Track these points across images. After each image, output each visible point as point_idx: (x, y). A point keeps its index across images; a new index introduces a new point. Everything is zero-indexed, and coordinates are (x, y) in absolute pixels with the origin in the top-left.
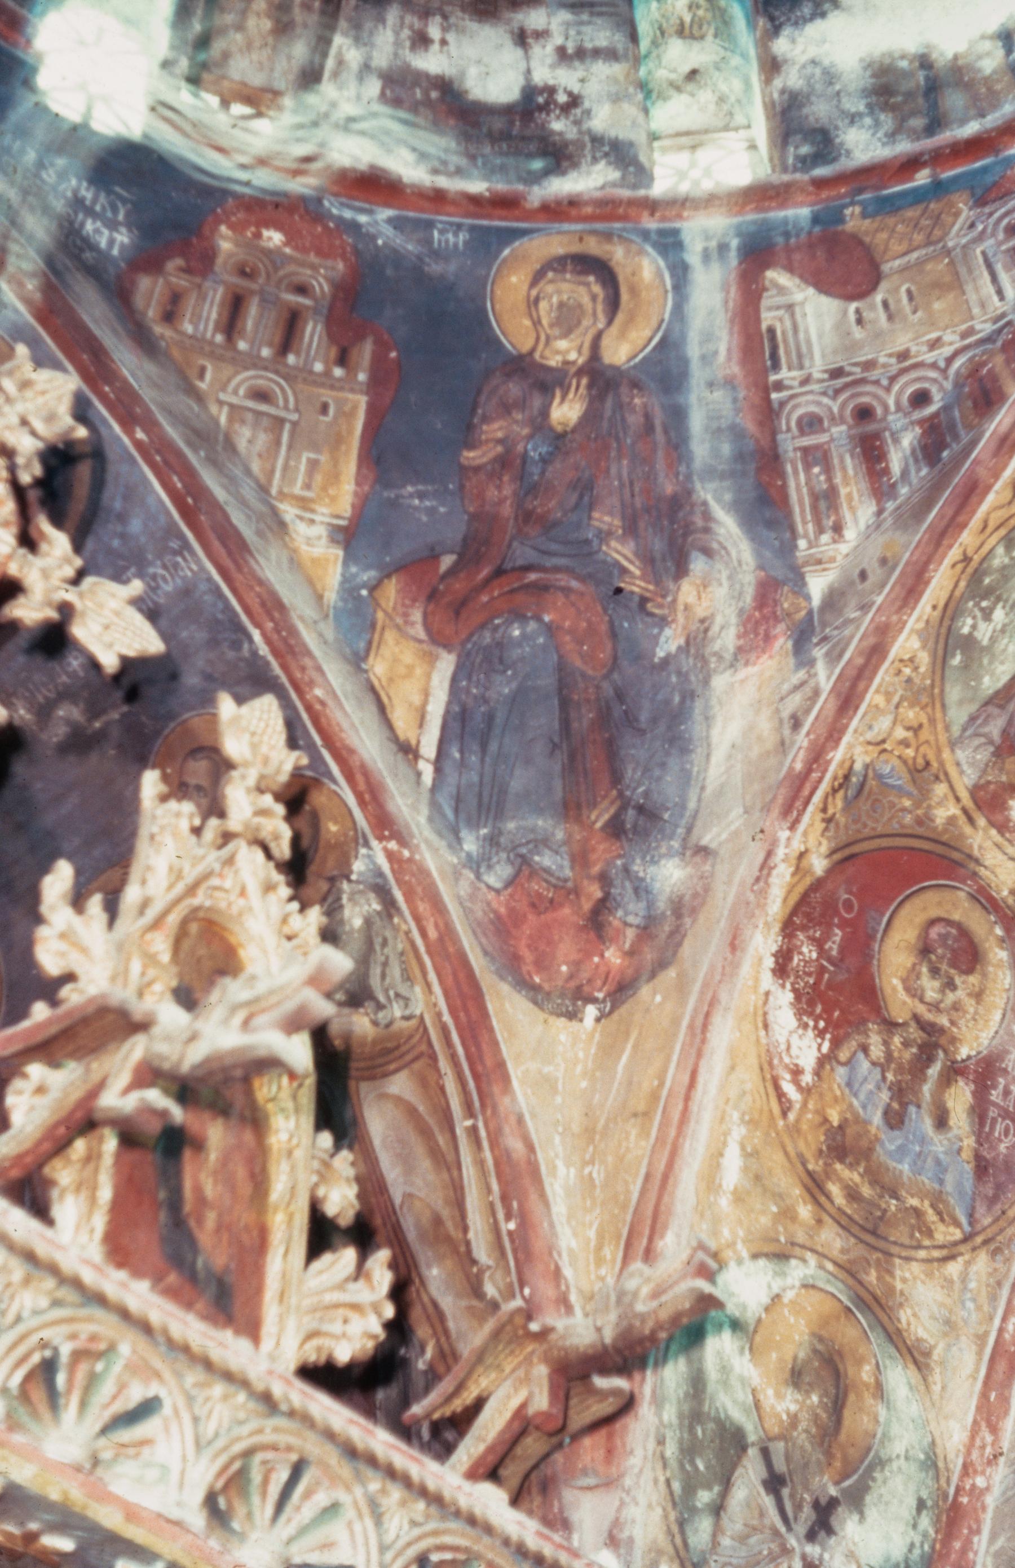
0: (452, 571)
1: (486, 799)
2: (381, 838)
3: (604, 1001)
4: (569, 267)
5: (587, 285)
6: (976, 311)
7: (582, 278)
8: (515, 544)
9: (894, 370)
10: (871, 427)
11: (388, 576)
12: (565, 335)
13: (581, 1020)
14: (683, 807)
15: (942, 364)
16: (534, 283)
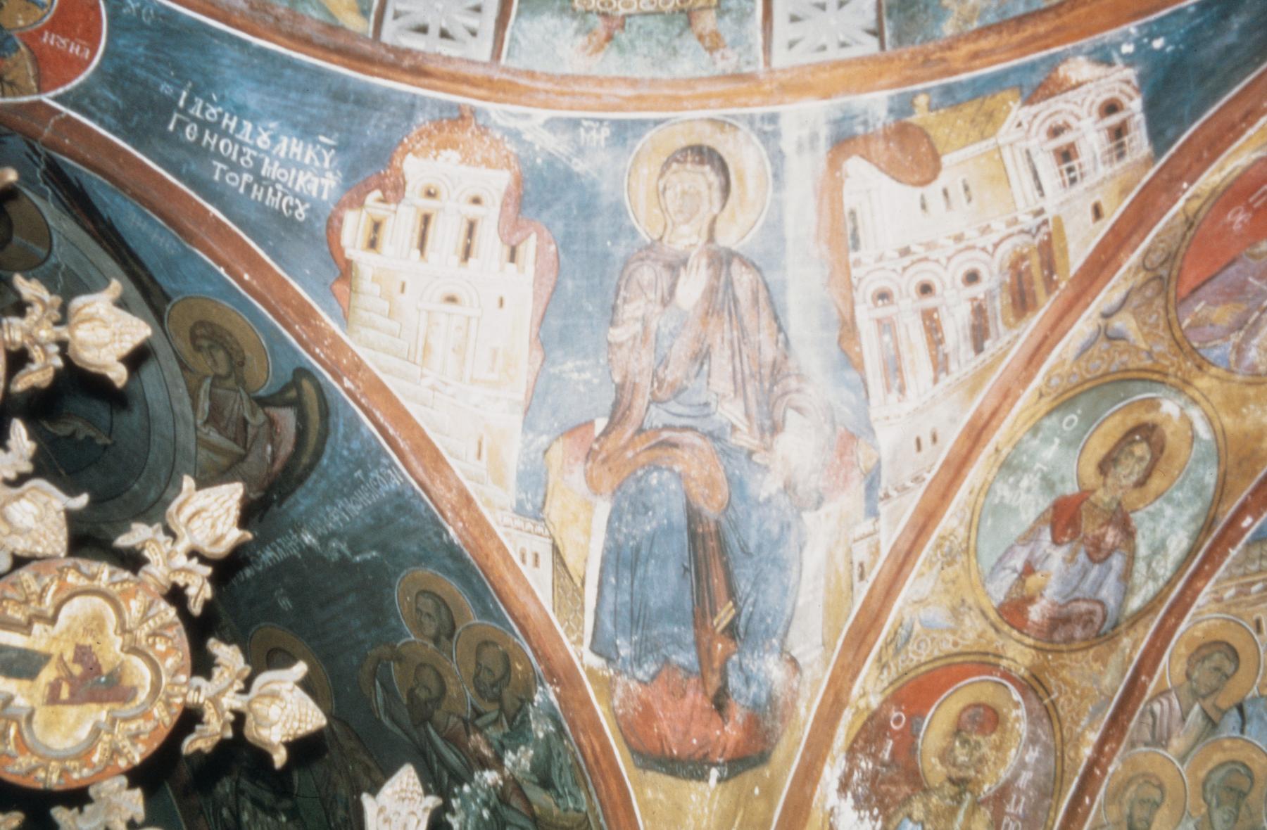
0: (606, 433)
1: (636, 614)
2: (552, 683)
3: (723, 765)
4: (689, 158)
5: (703, 174)
6: (1021, 204)
7: (699, 168)
8: (652, 407)
9: (950, 252)
10: (929, 302)
11: (557, 439)
12: (687, 221)
13: (707, 781)
14: (783, 612)
15: (990, 249)
16: (662, 174)
